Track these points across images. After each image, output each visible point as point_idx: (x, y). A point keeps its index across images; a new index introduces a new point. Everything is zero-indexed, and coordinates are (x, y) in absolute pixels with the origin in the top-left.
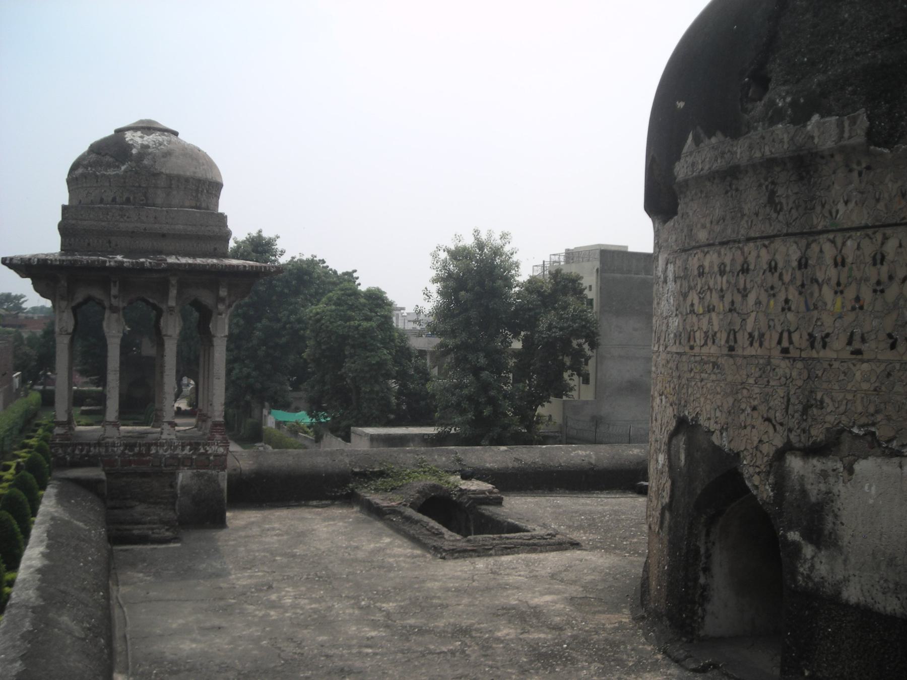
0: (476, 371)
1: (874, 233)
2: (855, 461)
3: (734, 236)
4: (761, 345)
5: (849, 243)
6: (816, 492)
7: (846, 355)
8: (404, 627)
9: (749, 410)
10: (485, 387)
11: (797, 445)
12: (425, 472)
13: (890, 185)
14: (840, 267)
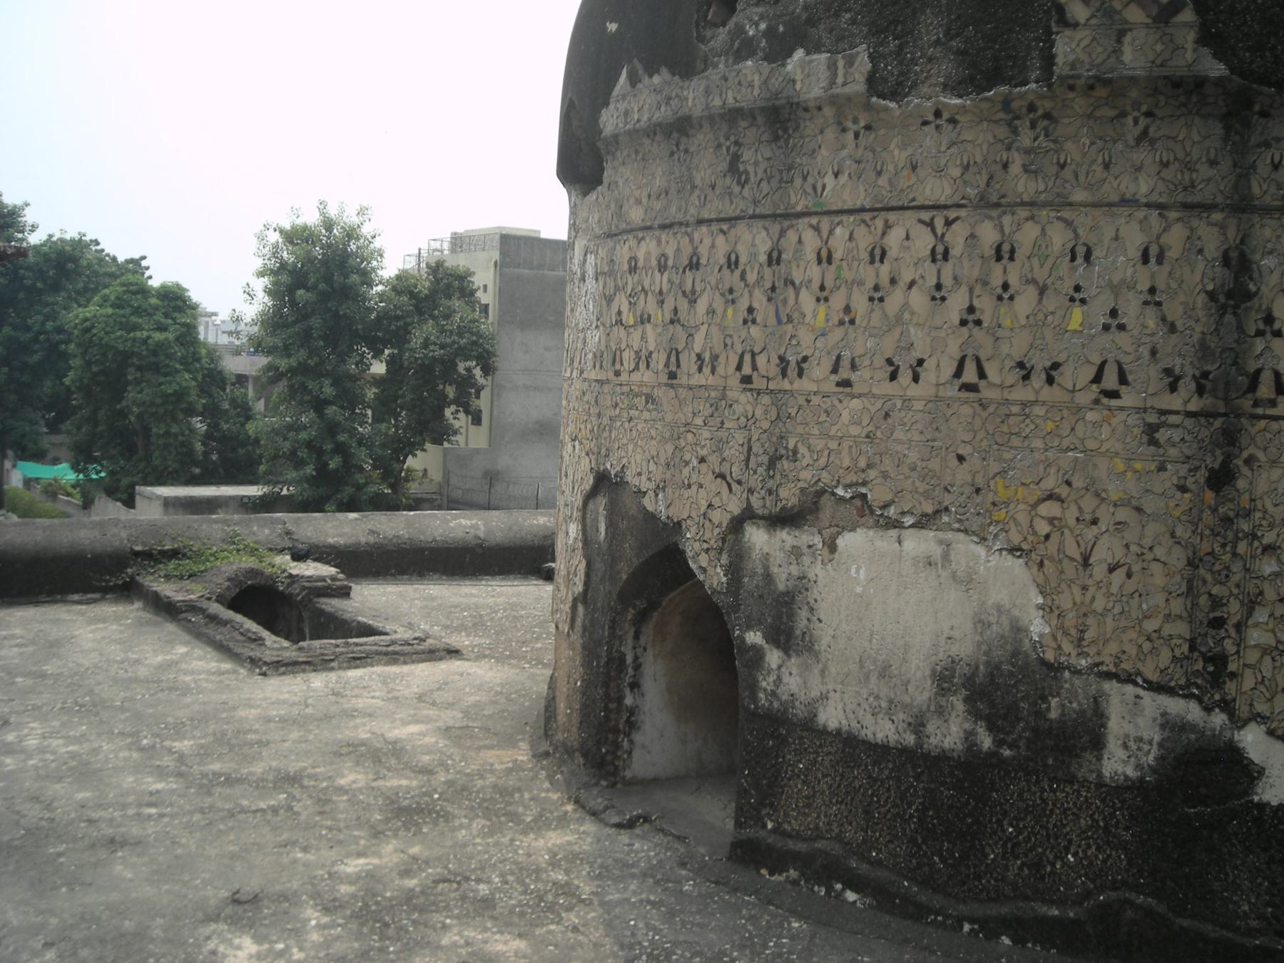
0: (319, 405)
1: (874, 218)
2: (839, 534)
3: (680, 217)
4: (713, 372)
5: (838, 230)
6: (784, 576)
7: (829, 386)
8: (204, 775)
9: (695, 462)
11: (760, 512)
12: (238, 550)
13: (896, 152)
14: (825, 265)
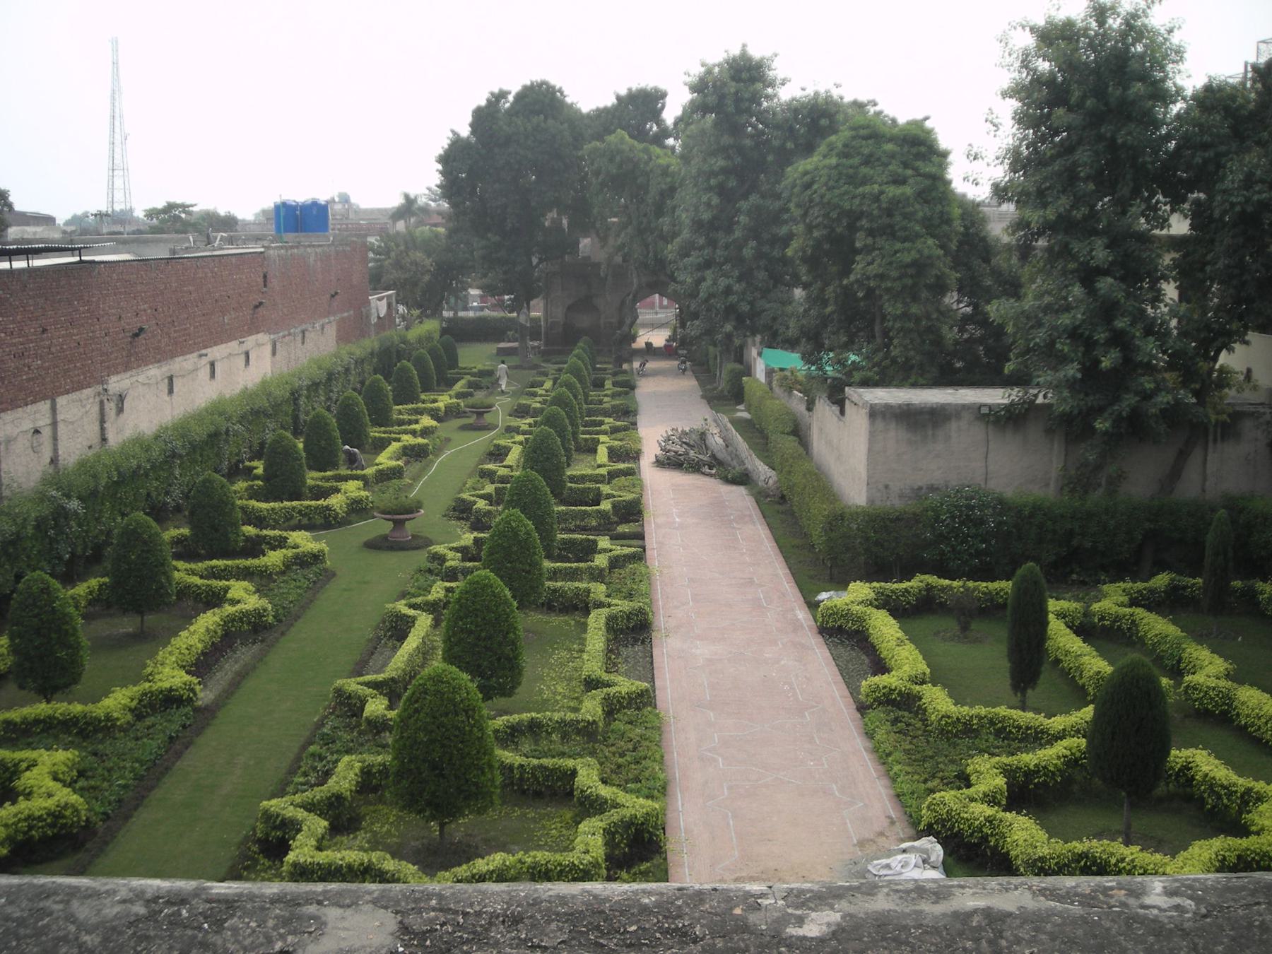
0: (1088, 276)
10: (1108, 310)
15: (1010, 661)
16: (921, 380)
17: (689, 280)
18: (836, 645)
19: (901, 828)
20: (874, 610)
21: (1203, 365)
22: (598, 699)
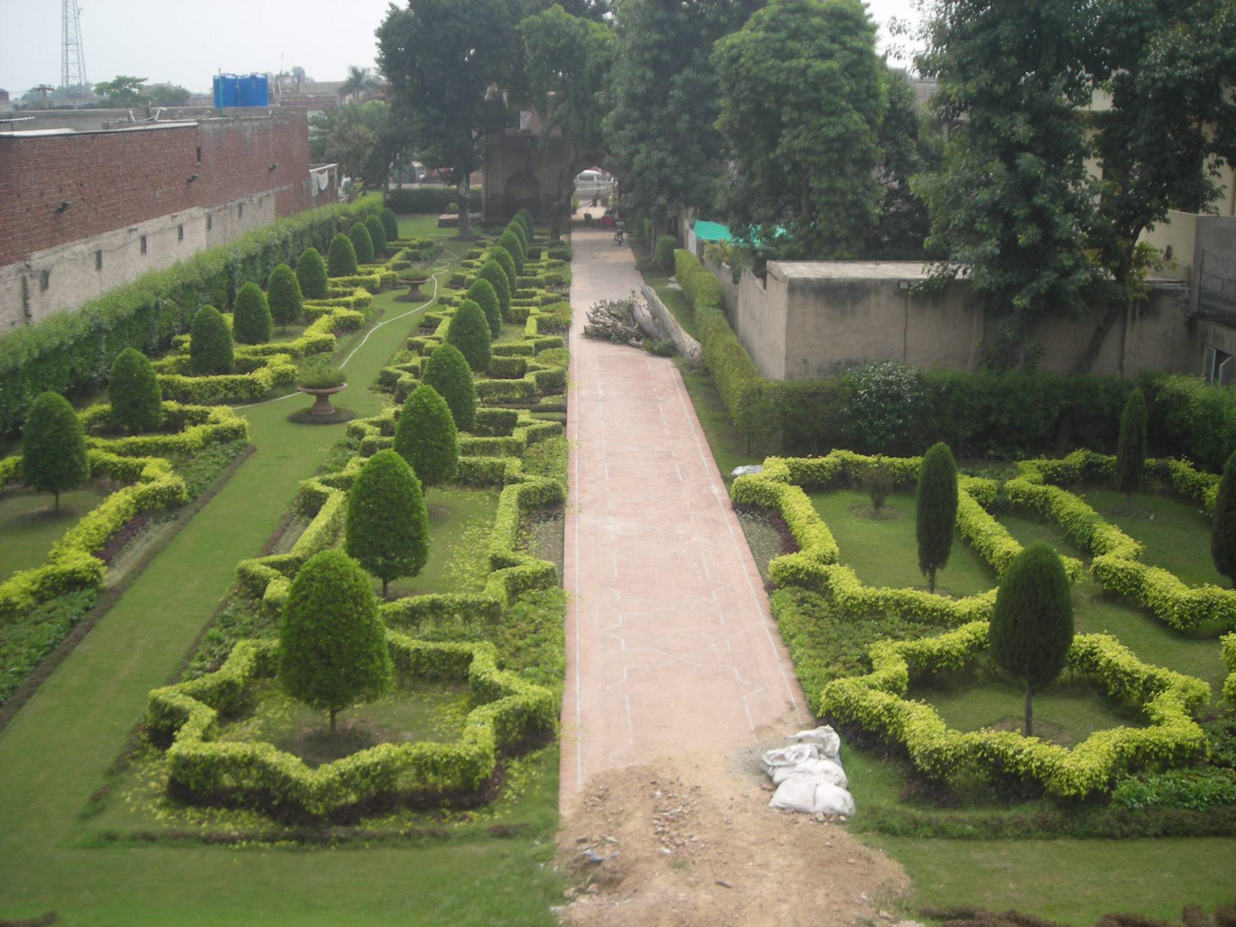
0: (1009, 151)
15: (919, 540)
16: (846, 254)
17: (623, 153)
18: (748, 522)
19: (802, 715)
20: (788, 487)
21: (1122, 244)
22: (502, 580)
